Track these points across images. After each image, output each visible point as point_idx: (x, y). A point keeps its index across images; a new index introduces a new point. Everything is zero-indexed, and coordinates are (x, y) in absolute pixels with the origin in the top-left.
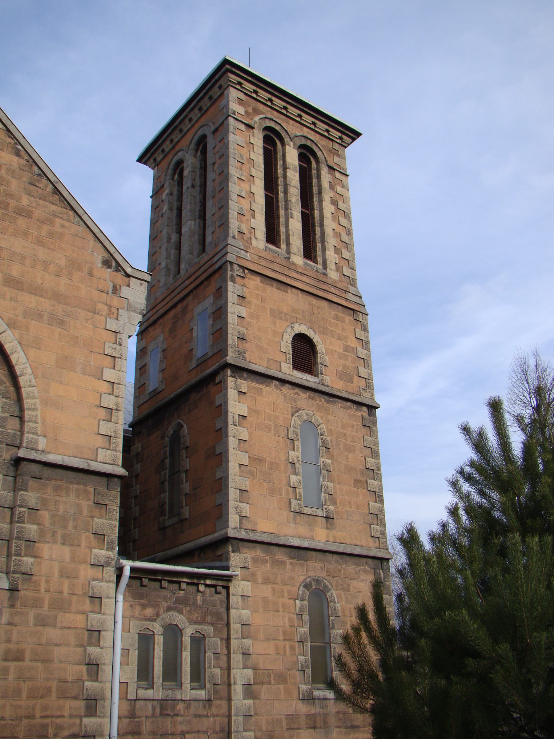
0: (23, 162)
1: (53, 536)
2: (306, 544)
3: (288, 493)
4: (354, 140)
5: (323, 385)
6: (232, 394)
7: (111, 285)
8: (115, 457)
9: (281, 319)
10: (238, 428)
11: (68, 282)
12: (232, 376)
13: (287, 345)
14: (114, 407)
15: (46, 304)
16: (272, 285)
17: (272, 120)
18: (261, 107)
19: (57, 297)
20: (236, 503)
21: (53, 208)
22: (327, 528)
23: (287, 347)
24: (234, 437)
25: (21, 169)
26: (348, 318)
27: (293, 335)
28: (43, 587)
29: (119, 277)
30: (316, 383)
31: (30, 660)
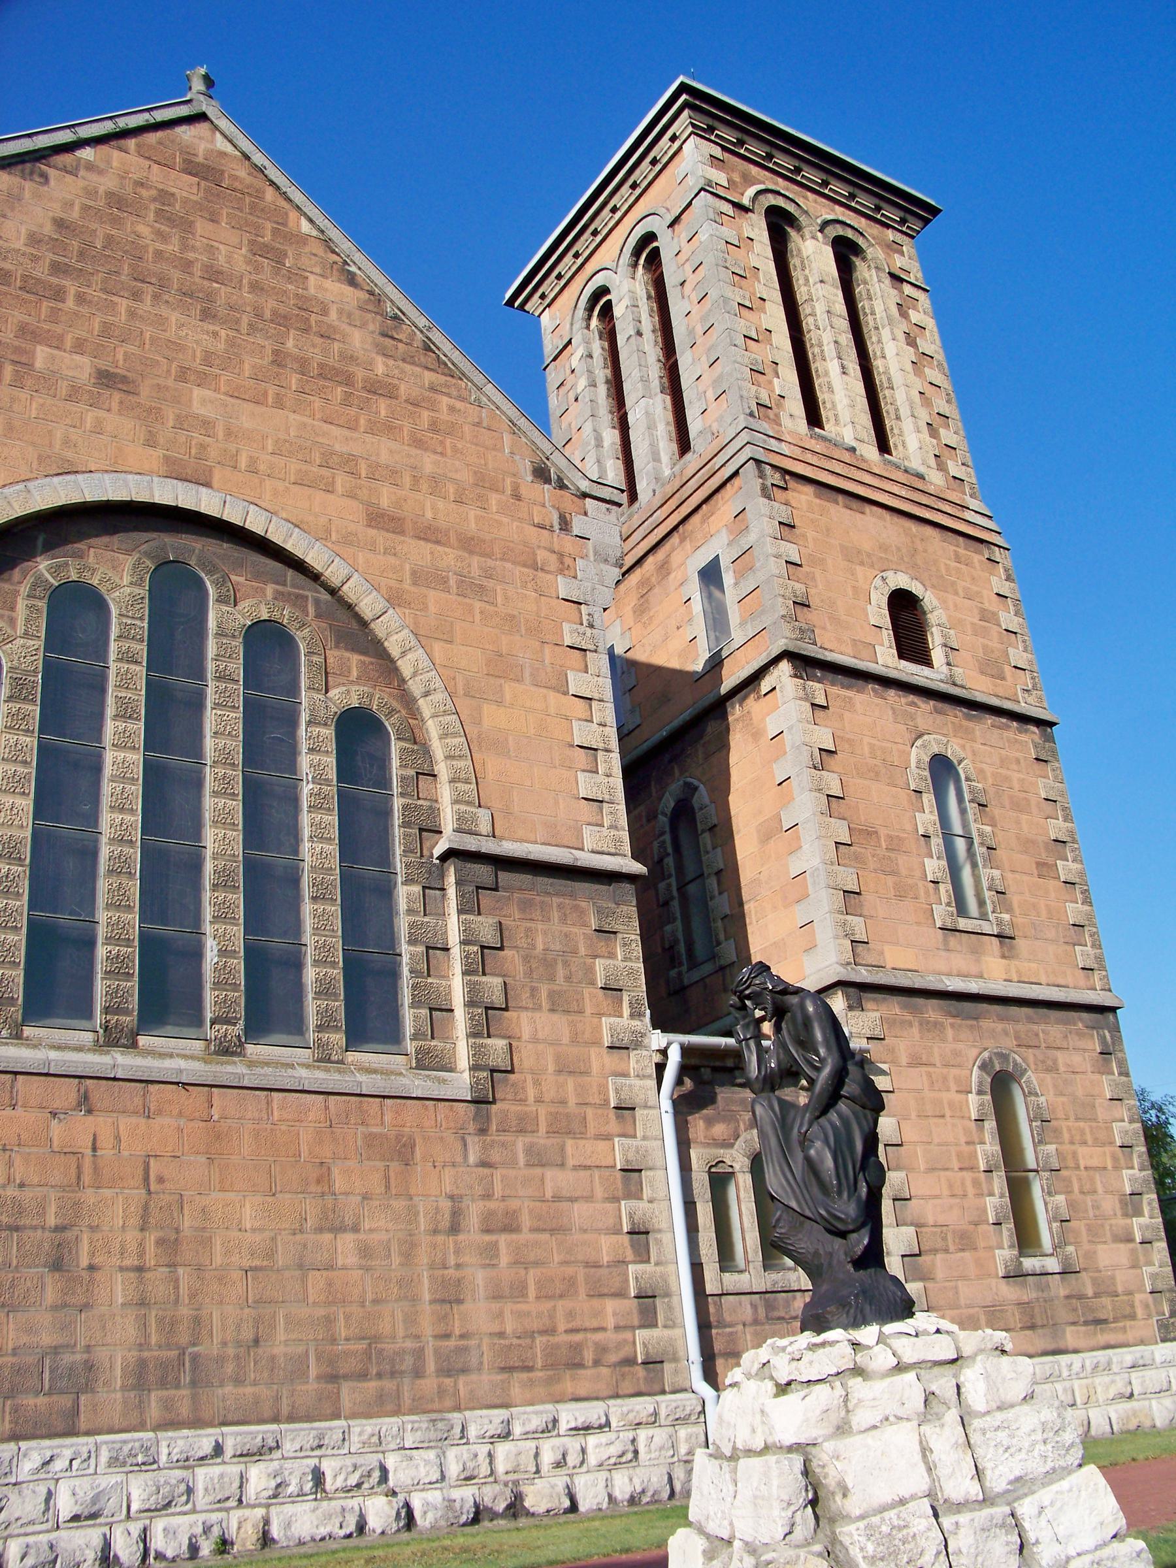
0: (364, 296)
1: (533, 996)
2: (973, 987)
3: (927, 892)
4: (926, 222)
5: (955, 685)
8: (618, 841)
9: (862, 563)
11: (480, 512)
13: (879, 613)
15: (449, 557)
17: (778, 193)
18: (754, 170)
19: (469, 544)
20: (841, 917)
21: (429, 377)
22: (1003, 957)
25: (360, 308)
27: (887, 593)
28: (531, 1093)
29: (568, 501)
31: (533, 1230)
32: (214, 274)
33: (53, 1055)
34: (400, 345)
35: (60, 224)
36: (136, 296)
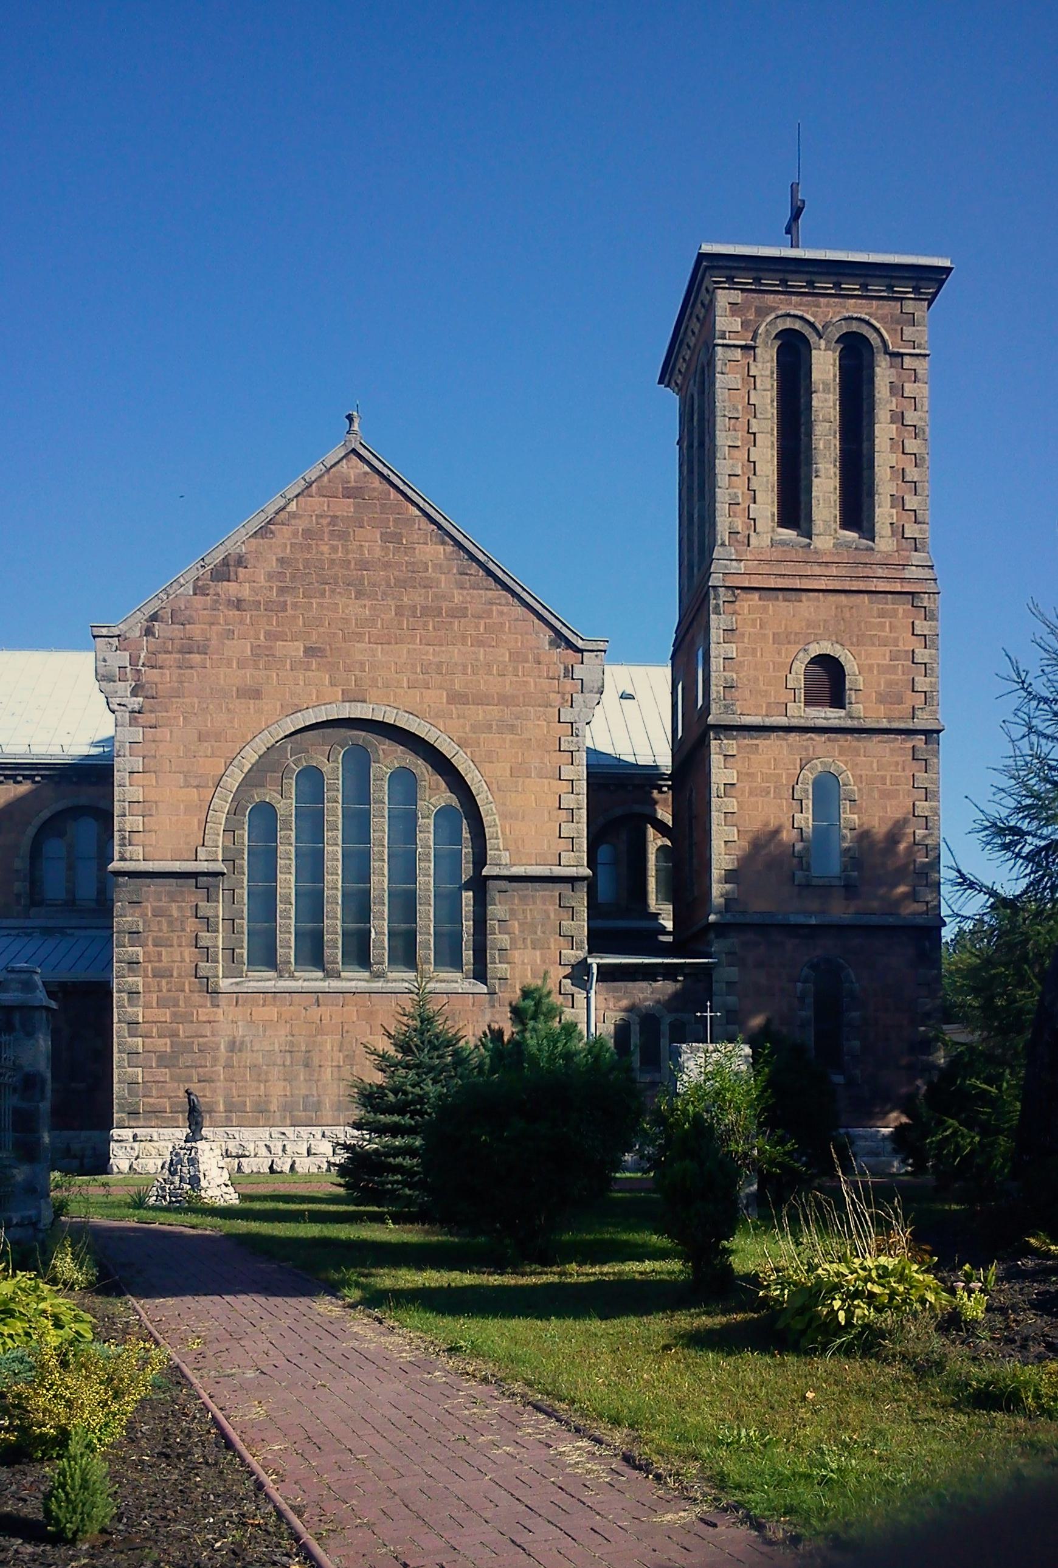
5: (852, 718)
6: (716, 760)
7: (562, 667)
9: (789, 643)
10: (725, 799)
12: (715, 739)
13: (798, 678)
14: (575, 807)
15: (494, 711)
16: (777, 599)
17: (789, 315)
19: (504, 700)
20: (721, 885)
21: (490, 593)
22: (847, 899)
23: (798, 679)
24: (719, 811)
26: (903, 608)
30: (840, 718)
32: (364, 565)
33: (306, 984)
34: (472, 577)
35: (281, 561)
36: (323, 594)
